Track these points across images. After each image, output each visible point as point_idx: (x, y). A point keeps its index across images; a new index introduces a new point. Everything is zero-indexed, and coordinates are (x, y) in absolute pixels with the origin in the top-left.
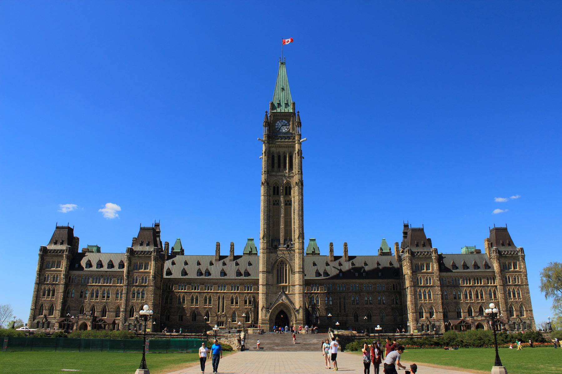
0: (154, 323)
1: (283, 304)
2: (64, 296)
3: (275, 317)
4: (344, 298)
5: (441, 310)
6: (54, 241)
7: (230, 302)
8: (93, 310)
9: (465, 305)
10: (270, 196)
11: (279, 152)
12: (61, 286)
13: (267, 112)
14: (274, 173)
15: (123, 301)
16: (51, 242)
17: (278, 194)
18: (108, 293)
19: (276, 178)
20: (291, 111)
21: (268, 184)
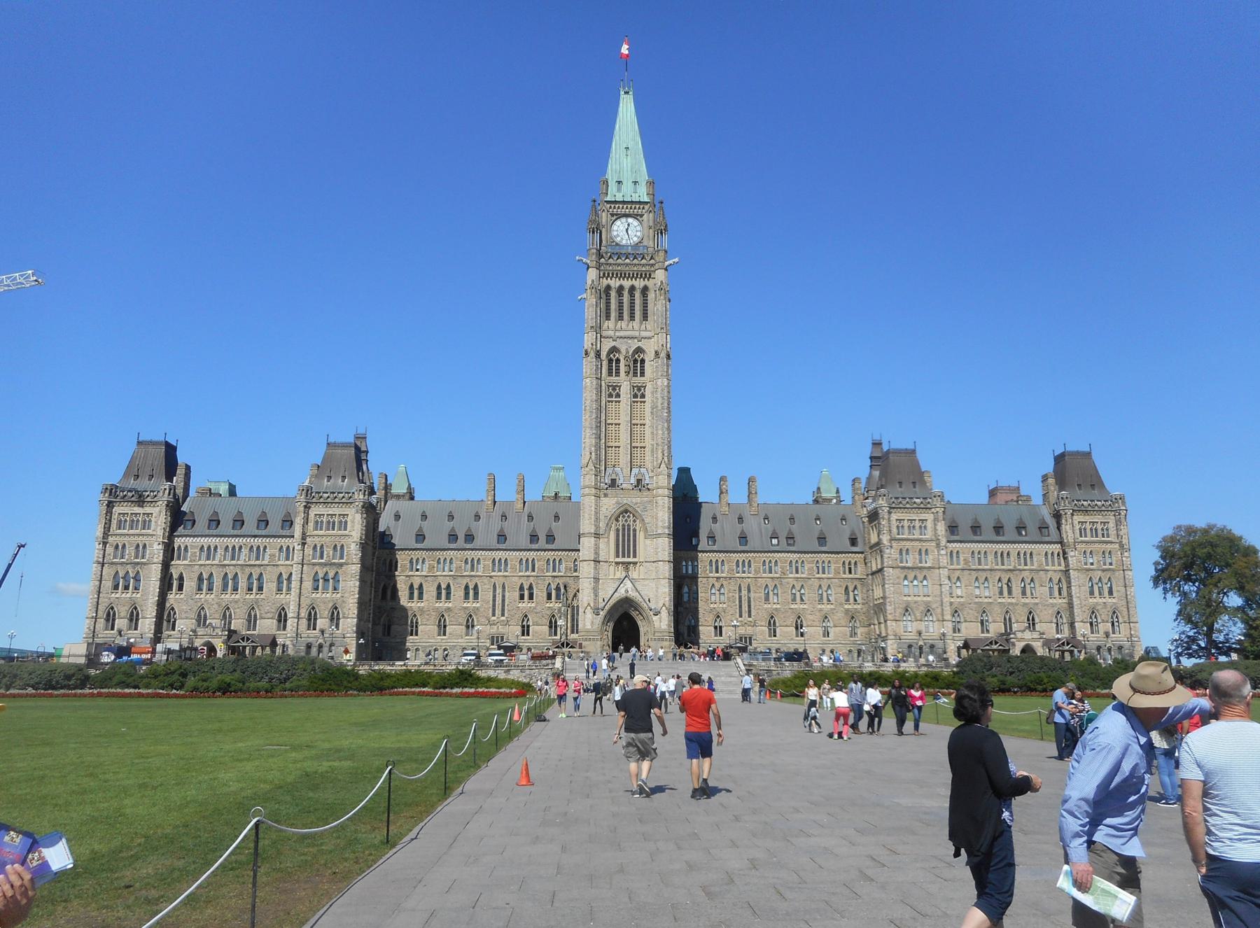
0: (362, 641)
4: (749, 591)
5: (948, 617)
7: (517, 594)
8: (226, 616)
9: (997, 609)
15: (293, 595)
16: (126, 475)
17: (618, 374)
20: (646, 200)
21: (598, 355)
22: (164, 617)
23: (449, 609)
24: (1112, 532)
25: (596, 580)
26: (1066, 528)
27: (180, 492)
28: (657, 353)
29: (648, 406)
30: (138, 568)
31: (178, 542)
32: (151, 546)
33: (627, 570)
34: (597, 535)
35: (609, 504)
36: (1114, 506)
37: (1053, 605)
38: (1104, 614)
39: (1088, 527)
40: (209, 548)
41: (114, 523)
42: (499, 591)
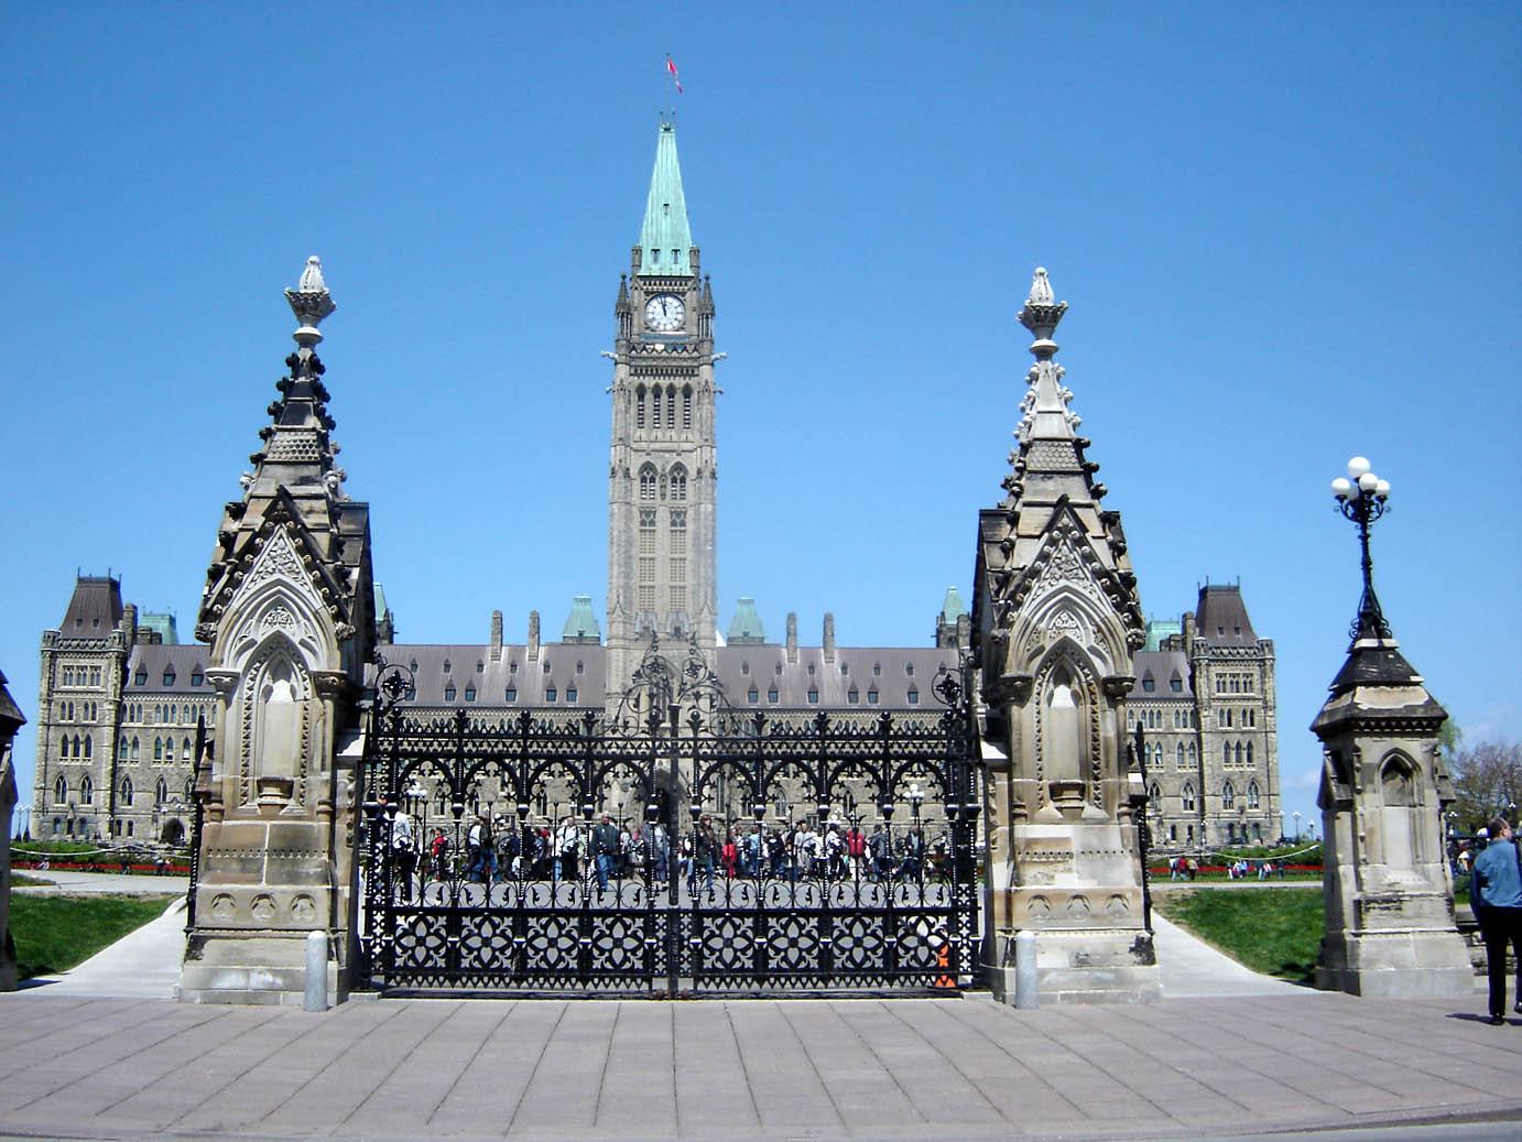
2: (115, 755)
6: (76, 615)
12: (106, 730)
13: (624, 277)
16: (68, 619)
20: (690, 273)
22: (121, 787)
24: (1257, 685)
26: (1201, 681)
27: (128, 638)
28: (699, 472)
29: (689, 537)
30: (88, 731)
31: (127, 701)
35: (637, 657)
36: (1261, 655)
37: (1181, 776)
38: (1240, 786)
39: (1228, 680)
40: (166, 707)
41: (59, 677)
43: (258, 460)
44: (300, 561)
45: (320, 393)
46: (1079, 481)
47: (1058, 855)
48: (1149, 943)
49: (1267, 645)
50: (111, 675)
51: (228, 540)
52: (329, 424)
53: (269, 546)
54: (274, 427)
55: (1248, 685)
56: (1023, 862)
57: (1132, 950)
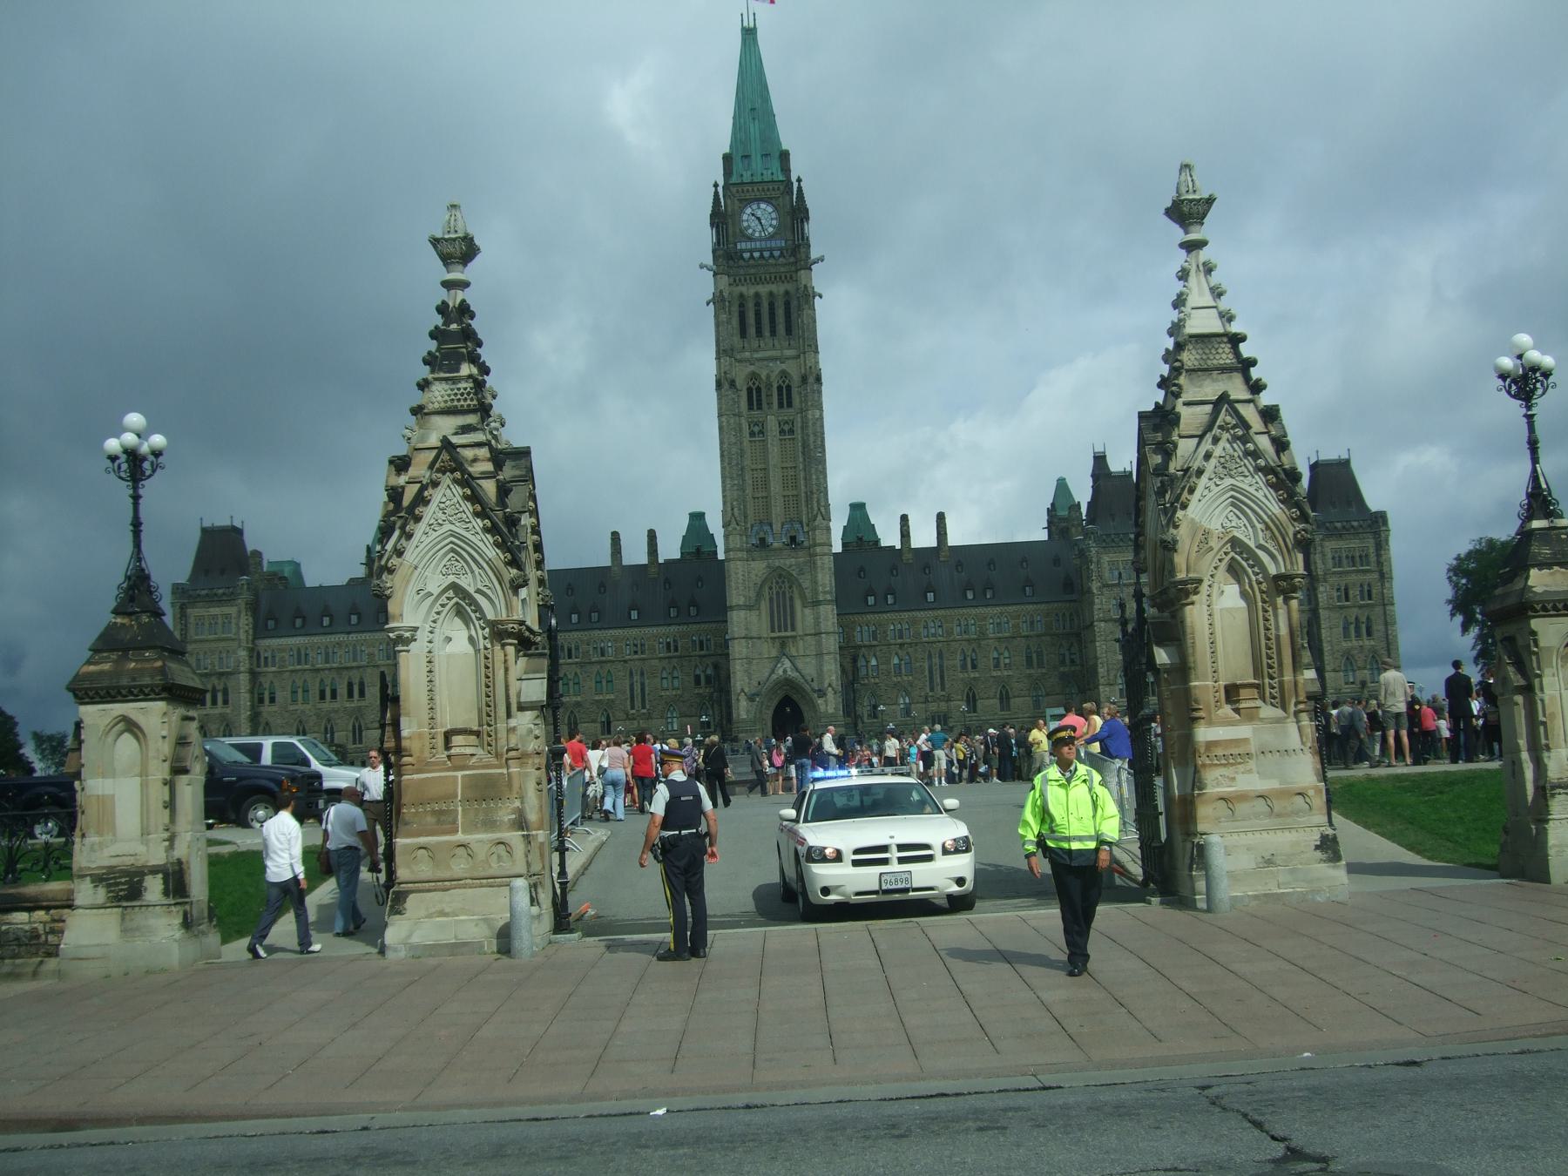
1: (788, 682)
2: (252, 701)
3: (770, 713)
10: (739, 415)
11: (757, 295)
12: (242, 677)
14: (747, 354)
17: (760, 407)
18: (362, 685)
19: (752, 368)
23: (578, 704)
24: (1373, 558)
25: (749, 660)
28: (804, 379)
32: (234, 652)
33: (783, 643)
34: (749, 608)
35: (759, 567)
42: (637, 678)
43: (418, 411)
44: (468, 507)
45: (469, 335)
46: (1238, 379)
47: (1236, 755)
48: (1334, 839)
49: (1380, 519)
50: (245, 621)
51: (395, 494)
52: (485, 370)
53: (437, 496)
54: (430, 377)
55: (1364, 558)
56: (1204, 765)
57: (1317, 847)
